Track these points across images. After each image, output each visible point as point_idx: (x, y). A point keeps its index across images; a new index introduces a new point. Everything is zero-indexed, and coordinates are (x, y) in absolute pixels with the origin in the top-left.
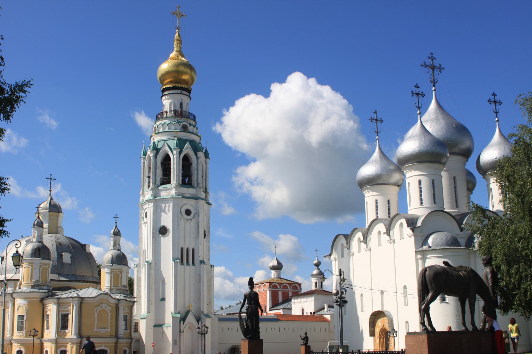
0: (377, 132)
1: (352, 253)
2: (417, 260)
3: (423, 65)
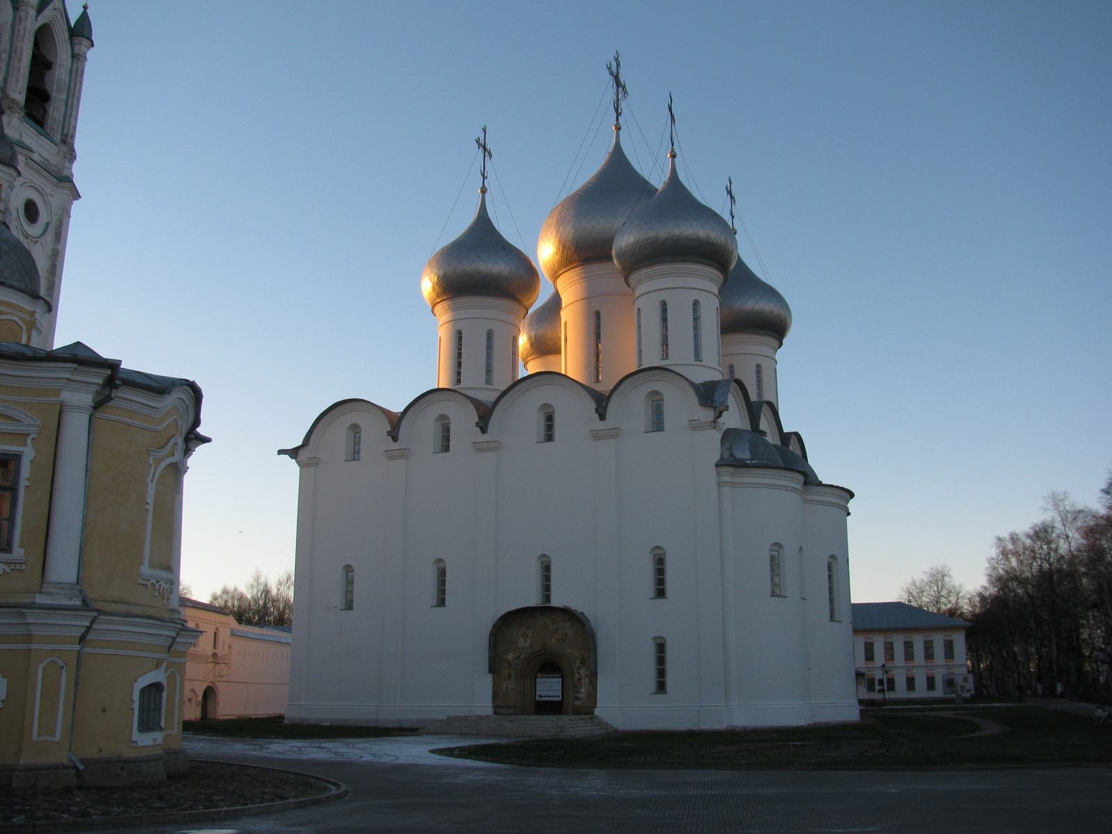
0: (484, 178)
2: (720, 484)
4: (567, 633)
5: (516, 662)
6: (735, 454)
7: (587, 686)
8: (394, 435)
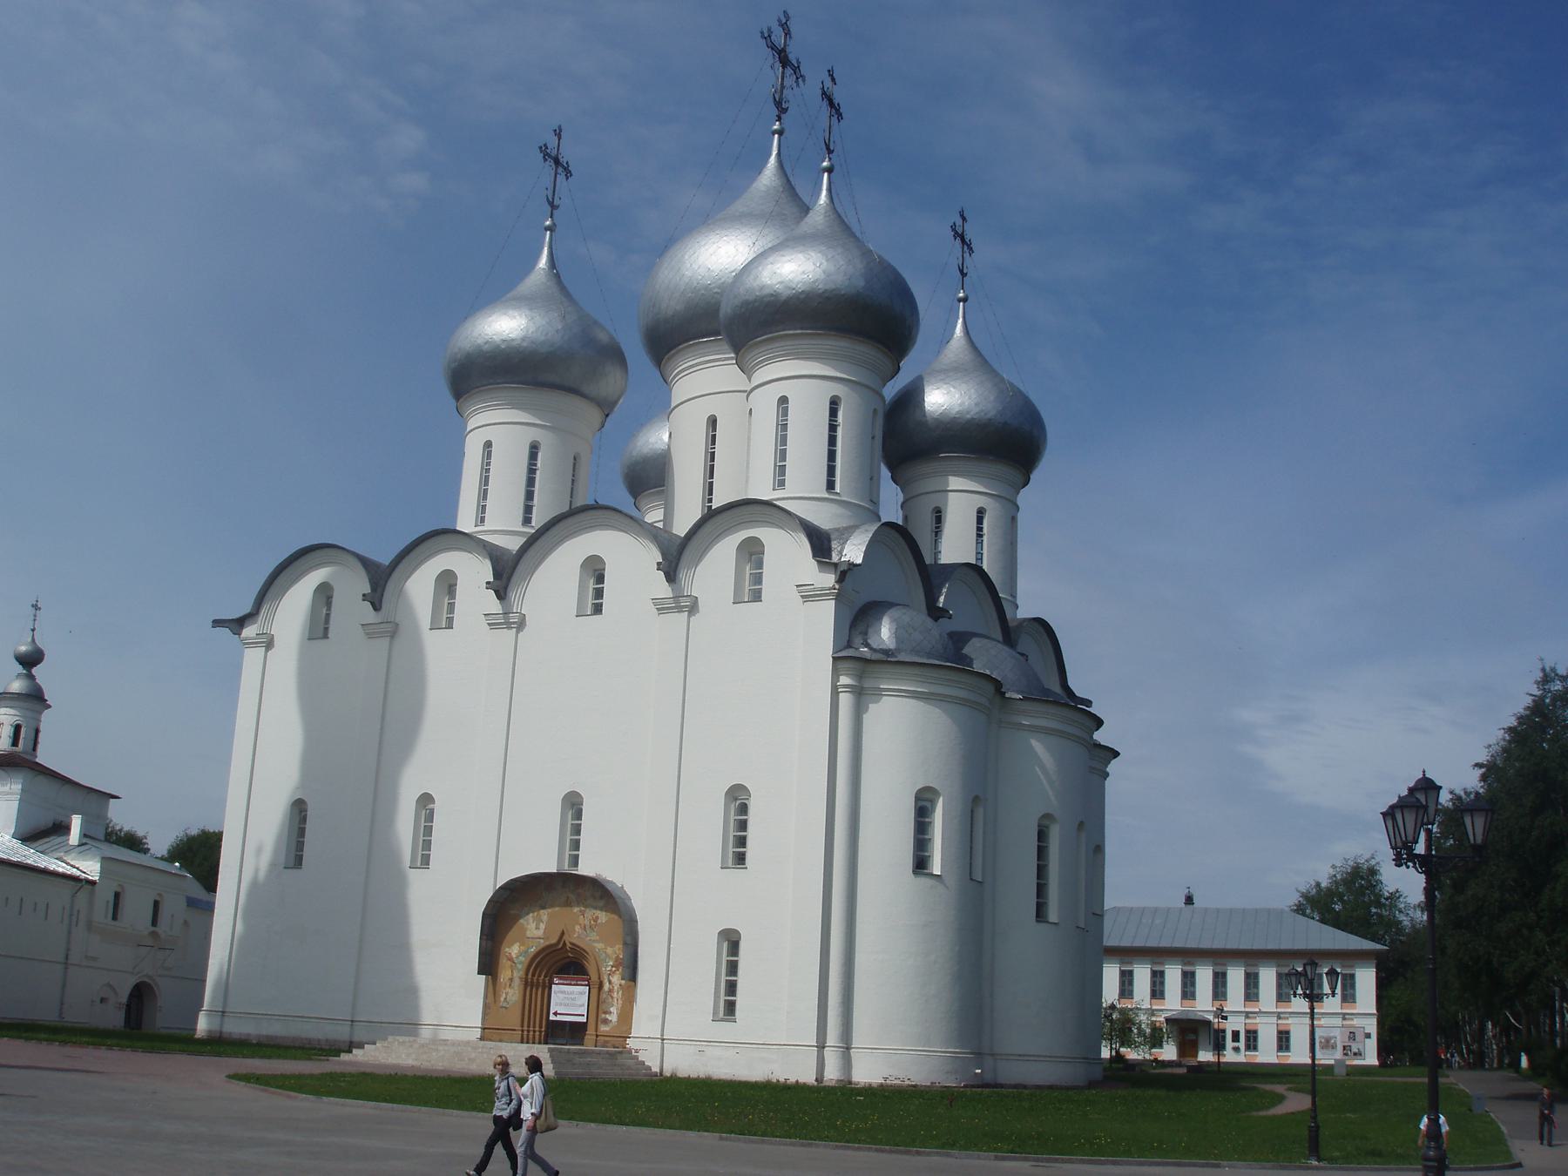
0: (553, 206)
1: (694, 599)
3: (766, 35)
4: (597, 918)
5: (522, 959)
6: (869, 641)
7: (620, 1002)
8: (375, 599)
